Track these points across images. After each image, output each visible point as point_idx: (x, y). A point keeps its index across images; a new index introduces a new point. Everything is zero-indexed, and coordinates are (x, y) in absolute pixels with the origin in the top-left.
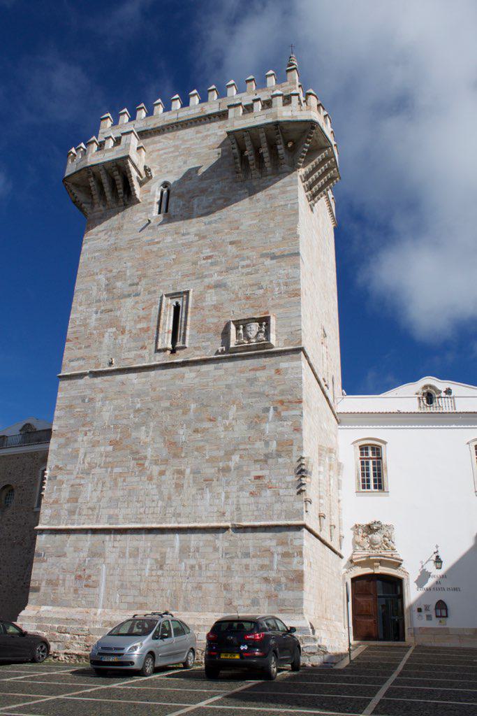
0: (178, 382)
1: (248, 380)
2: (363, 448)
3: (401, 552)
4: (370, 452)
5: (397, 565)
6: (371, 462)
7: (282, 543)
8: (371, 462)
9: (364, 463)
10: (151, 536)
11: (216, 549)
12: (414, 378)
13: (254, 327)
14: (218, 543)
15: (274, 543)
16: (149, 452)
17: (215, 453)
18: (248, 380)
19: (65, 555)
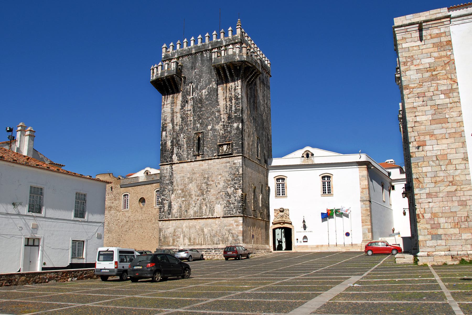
0: (201, 167)
1: (224, 167)
2: (278, 180)
3: (292, 218)
4: (281, 180)
5: (291, 224)
6: (281, 185)
7: (236, 222)
8: (281, 185)
9: (278, 185)
10: (196, 221)
11: (216, 224)
12: (302, 148)
13: (225, 147)
14: (217, 222)
15: (234, 222)
16: (193, 193)
17: (215, 193)
18: (224, 167)
19: (169, 228)
